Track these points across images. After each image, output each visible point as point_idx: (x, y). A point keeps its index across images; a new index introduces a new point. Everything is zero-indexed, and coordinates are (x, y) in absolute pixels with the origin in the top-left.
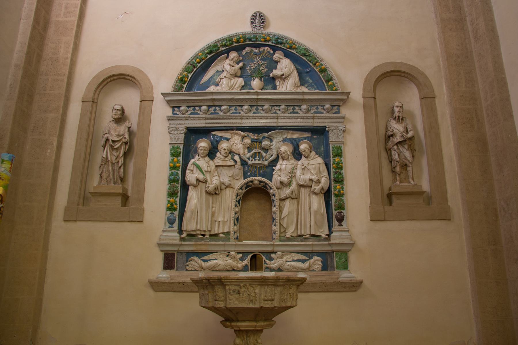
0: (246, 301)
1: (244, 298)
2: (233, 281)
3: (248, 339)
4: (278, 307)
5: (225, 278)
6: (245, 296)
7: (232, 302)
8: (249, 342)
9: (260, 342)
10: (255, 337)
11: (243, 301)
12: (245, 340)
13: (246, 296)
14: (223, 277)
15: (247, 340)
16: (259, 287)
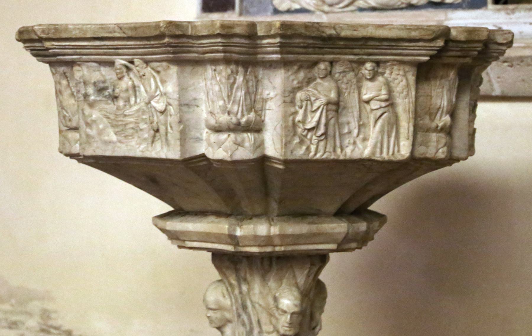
0: (141, 130)
1: (132, 120)
2: (82, 47)
3: (245, 288)
4: (286, 162)
5: (51, 36)
6: (135, 108)
7: (92, 132)
8: (249, 304)
9: (285, 308)
10: (272, 284)
11: (131, 131)
12: (237, 292)
13: (138, 111)
14: (43, 31)
15: (241, 293)
16: (174, 69)
